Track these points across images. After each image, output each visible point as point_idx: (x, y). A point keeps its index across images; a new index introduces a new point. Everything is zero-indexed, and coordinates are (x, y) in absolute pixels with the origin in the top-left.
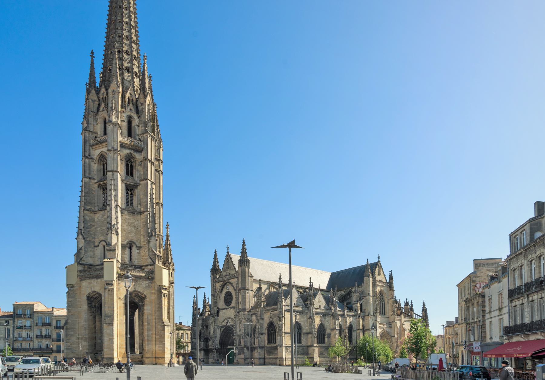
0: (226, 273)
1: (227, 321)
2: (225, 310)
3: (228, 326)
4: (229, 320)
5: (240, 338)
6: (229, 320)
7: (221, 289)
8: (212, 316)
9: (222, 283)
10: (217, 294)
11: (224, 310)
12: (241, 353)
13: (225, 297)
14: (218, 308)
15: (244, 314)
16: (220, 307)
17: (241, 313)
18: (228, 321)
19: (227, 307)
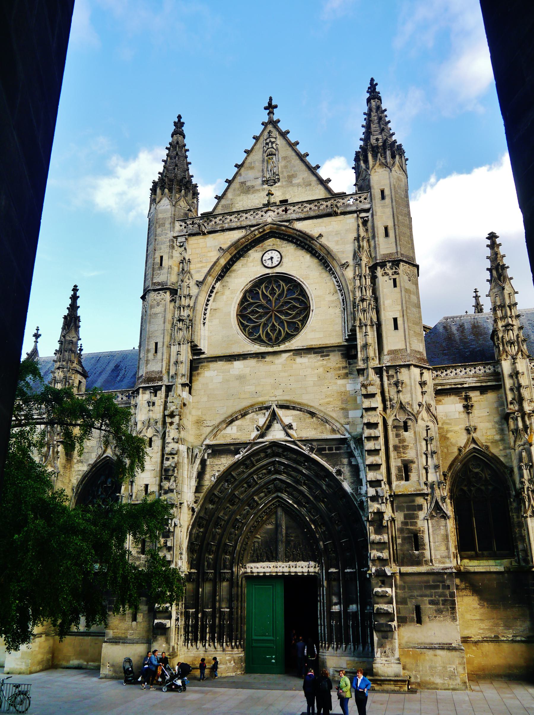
0: (270, 194)
1: (262, 419)
2: (252, 362)
3: (274, 444)
4: (280, 412)
5: (410, 518)
6: (280, 412)
7: (223, 262)
8: (159, 388)
9: (237, 235)
10: (199, 284)
11: (238, 364)
12: (427, 608)
13: (244, 299)
14: (196, 350)
15: (423, 384)
16: (203, 345)
17: (404, 375)
18: (274, 416)
19: (257, 348)
